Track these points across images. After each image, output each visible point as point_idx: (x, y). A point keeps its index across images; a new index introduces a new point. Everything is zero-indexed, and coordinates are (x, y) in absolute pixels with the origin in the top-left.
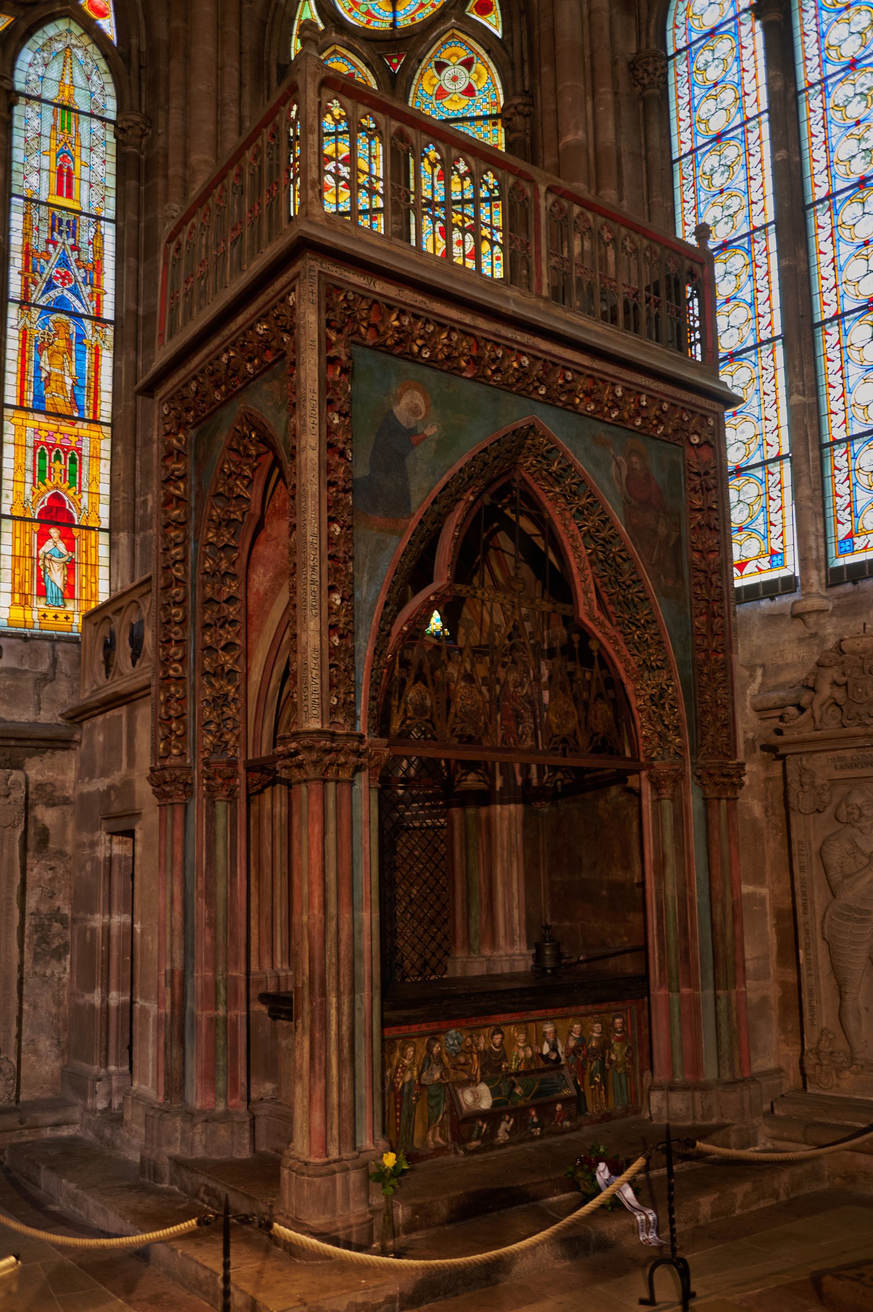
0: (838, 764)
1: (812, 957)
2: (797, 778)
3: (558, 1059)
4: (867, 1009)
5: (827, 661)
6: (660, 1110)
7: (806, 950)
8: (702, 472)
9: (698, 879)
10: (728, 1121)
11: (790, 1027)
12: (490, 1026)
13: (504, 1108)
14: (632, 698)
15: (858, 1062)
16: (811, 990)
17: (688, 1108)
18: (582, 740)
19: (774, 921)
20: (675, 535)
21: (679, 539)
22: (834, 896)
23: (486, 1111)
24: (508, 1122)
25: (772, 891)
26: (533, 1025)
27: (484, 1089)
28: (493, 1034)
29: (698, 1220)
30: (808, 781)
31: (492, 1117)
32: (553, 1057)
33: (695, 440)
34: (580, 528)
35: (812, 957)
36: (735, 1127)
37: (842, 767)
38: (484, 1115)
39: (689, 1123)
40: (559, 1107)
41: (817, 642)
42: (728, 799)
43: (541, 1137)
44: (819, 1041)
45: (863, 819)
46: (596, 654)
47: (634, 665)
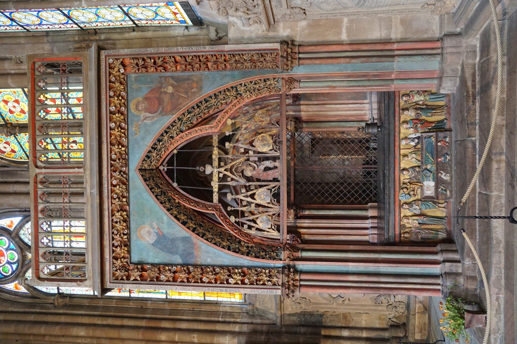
3: (418, 138)
6: (449, 90)
8: (137, 68)
10: (461, 62)
12: (400, 176)
13: (435, 175)
14: (252, 99)
17: (451, 80)
18: (274, 131)
20: (171, 81)
21: (172, 77)
23: (435, 184)
24: (442, 174)
26: (401, 150)
27: (426, 183)
28: (403, 174)
29: (503, 125)
31: (439, 182)
32: (416, 141)
33: (122, 71)
34: (177, 135)
36: (464, 60)
38: (437, 187)
39: (458, 80)
40: (439, 144)
43: (451, 156)
46: (233, 121)
47: (236, 101)
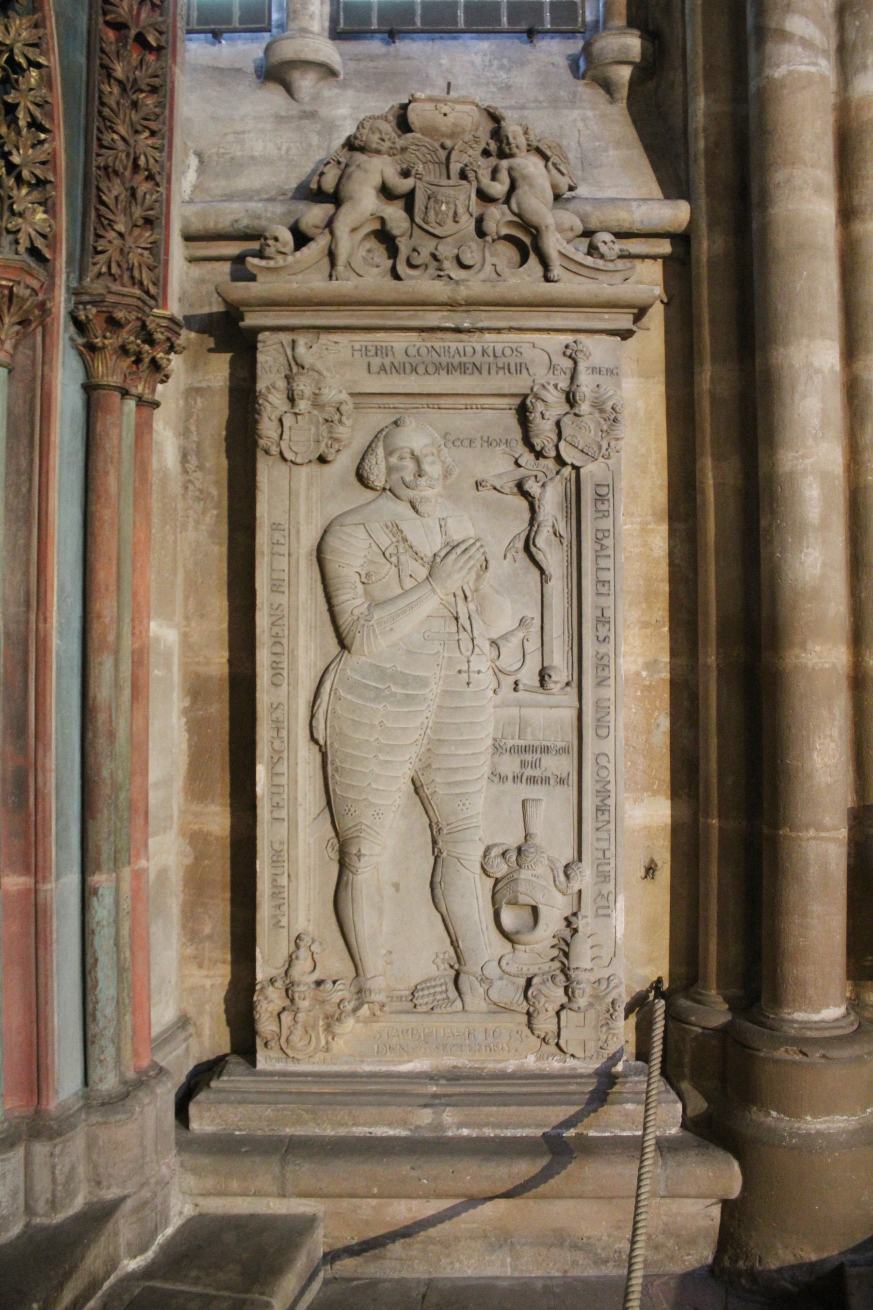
0: (376, 362)
1: (284, 780)
2: (282, 384)
4: (397, 887)
5: (375, 138)
7: (273, 765)
9: (62, 589)
11: (207, 930)
15: (375, 997)
16: (277, 853)
19: (187, 703)
22: (343, 645)
25: (185, 637)
30: (308, 391)
35: (284, 780)
37: (383, 368)
41: (318, 127)
42: (141, 401)
44: (291, 960)
45: (422, 481)
